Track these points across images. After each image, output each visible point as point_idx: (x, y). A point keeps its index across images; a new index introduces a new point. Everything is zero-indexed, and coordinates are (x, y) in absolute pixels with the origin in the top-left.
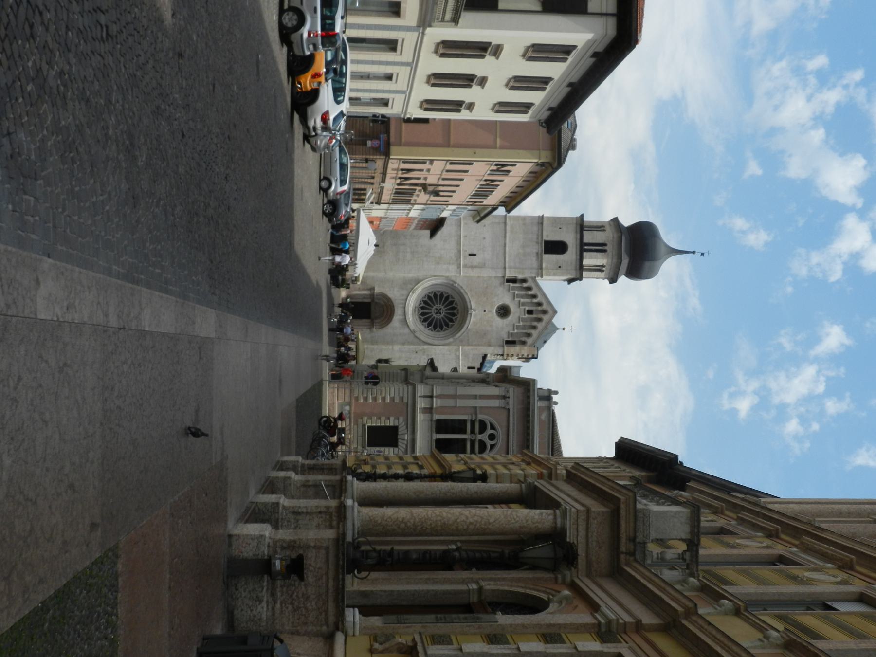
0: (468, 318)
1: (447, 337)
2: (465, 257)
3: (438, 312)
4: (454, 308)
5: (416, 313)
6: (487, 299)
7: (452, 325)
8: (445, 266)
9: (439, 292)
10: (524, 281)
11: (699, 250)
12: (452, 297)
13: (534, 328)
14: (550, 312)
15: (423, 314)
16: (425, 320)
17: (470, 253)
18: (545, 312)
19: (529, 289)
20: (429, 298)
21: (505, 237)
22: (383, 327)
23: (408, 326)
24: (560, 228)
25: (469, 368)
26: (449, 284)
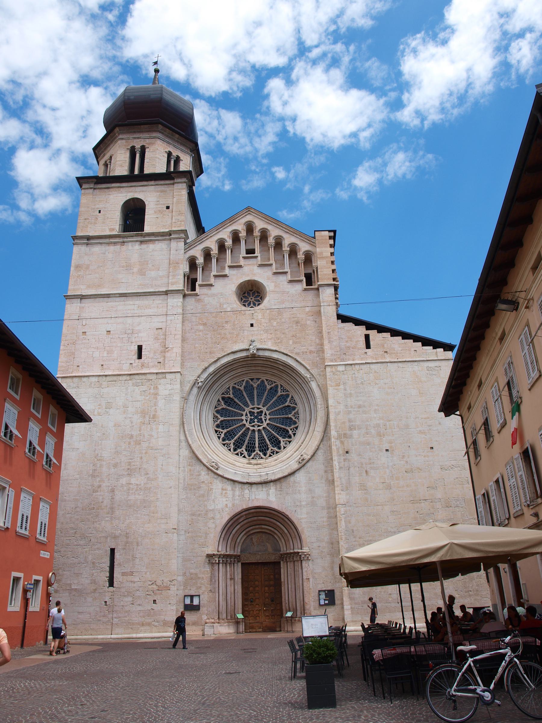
0: (267, 354)
1: (308, 394)
2: (143, 366)
3: (257, 416)
4: (249, 389)
6: (227, 322)
7: (284, 390)
8: (161, 403)
9: (215, 417)
12: (227, 392)
13: (278, 244)
15: (264, 449)
16: (277, 444)
17: (136, 356)
21: (108, 296)
24: (100, 212)
25: (368, 346)
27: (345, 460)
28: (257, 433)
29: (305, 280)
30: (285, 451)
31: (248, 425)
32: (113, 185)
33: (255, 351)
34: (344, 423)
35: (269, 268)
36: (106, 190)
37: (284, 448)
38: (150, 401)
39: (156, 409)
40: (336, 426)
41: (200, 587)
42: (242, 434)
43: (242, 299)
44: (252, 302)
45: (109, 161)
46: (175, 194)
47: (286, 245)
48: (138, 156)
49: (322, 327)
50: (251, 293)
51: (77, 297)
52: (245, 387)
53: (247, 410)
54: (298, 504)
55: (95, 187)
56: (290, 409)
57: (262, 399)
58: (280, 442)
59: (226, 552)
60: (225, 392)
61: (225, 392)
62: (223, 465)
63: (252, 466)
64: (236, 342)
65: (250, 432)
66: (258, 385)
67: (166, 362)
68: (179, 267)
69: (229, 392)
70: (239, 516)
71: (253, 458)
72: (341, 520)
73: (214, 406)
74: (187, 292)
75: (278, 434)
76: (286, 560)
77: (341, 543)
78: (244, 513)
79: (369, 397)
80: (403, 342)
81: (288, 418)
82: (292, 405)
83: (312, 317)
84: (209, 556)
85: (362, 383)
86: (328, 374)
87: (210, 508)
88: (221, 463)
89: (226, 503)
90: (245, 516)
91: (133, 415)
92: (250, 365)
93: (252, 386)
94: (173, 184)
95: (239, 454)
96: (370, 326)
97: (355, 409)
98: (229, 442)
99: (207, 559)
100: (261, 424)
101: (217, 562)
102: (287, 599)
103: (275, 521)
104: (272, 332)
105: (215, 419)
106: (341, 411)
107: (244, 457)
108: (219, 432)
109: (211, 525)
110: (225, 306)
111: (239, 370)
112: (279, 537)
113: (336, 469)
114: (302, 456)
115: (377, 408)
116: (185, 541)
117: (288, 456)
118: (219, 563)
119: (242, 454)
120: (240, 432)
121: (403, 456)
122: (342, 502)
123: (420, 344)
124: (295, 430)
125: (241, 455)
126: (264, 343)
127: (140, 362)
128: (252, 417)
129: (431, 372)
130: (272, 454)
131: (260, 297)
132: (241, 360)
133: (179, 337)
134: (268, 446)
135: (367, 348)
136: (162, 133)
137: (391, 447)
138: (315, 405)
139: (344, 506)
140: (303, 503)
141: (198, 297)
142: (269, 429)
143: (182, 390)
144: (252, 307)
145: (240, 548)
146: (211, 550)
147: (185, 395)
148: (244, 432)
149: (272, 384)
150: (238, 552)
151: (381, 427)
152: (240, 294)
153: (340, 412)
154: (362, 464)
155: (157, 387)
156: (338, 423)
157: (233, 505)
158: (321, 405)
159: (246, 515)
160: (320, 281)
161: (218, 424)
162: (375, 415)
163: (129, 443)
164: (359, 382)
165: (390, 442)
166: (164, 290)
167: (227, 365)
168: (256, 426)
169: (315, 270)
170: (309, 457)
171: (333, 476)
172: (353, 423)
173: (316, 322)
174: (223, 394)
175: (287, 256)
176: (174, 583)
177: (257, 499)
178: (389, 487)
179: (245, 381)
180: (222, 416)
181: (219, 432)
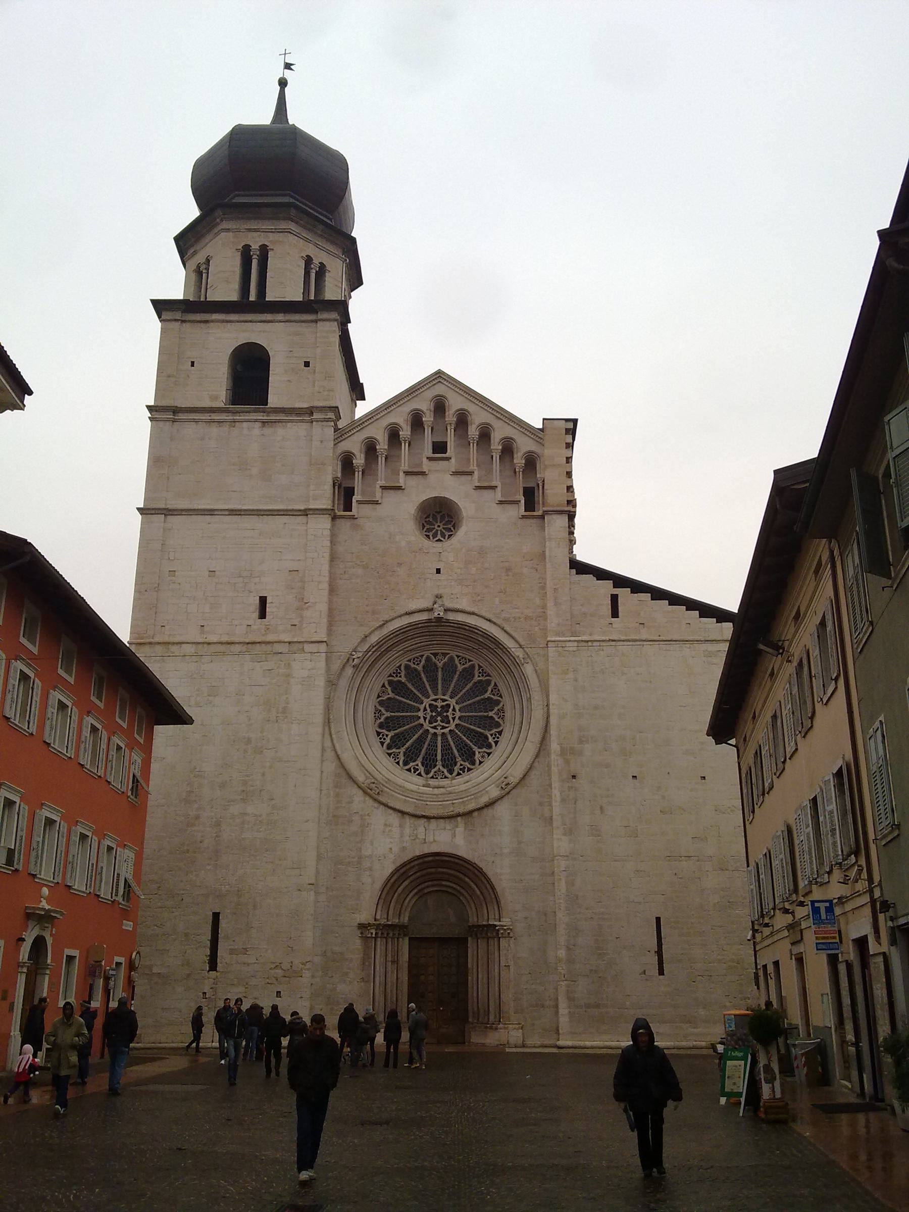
0: (460, 618)
1: (520, 685)
6: (400, 564)
7: (483, 673)
9: (378, 713)
10: (347, 462)
11: (280, 72)
12: (397, 673)
13: (485, 435)
14: (440, 390)
15: (450, 764)
16: (469, 756)
17: (257, 614)
18: (440, 407)
19: (371, 448)
20: (396, 742)
21: (211, 512)
22: (493, 888)
23: (491, 804)
24: (193, 364)
25: (615, 614)
28: (439, 738)
29: (523, 502)
30: (481, 769)
31: (426, 726)
32: (215, 316)
33: (442, 614)
35: (469, 477)
36: (202, 325)
37: (480, 764)
38: (279, 686)
39: (287, 698)
41: (347, 974)
43: (424, 526)
44: (439, 532)
45: (204, 266)
46: (318, 340)
47: (497, 440)
48: (255, 263)
49: (546, 579)
51: (159, 512)
52: (424, 667)
53: (427, 702)
55: (183, 319)
56: (491, 703)
58: (474, 753)
59: (388, 921)
60: (394, 673)
61: (394, 673)
62: (387, 788)
63: (431, 789)
65: (430, 736)
66: (444, 664)
67: (304, 625)
70: (408, 867)
71: (432, 777)
72: (560, 879)
74: (339, 513)
76: (476, 935)
77: (560, 915)
78: (416, 862)
80: (670, 610)
81: (487, 716)
82: (495, 698)
84: (362, 927)
86: (550, 655)
87: (366, 854)
88: (384, 784)
89: (390, 846)
91: (252, 707)
92: (432, 633)
93: (435, 664)
94: (316, 321)
95: (413, 770)
98: (398, 751)
99: (359, 932)
100: (447, 725)
101: (374, 936)
102: (475, 995)
103: (461, 876)
105: (377, 715)
107: (420, 774)
108: (383, 735)
109: (366, 879)
110: (397, 538)
111: (417, 640)
112: (467, 900)
113: (556, 801)
114: (505, 778)
116: (326, 903)
117: (486, 775)
118: (376, 938)
119: (416, 770)
121: (659, 788)
123: (696, 613)
124: (497, 735)
125: (415, 772)
127: (263, 623)
131: (452, 524)
132: (420, 625)
133: (325, 586)
134: (455, 760)
135: (612, 617)
136: (297, 223)
138: (529, 699)
139: (566, 858)
140: (506, 851)
141: (356, 521)
142: (459, 733)
143: (328, 669)
144: (439, 540)
145: (407, 914)
146: (365, 917)
148: (420, 736)
149: (466, 662)
150: (405, 919)
152: (421, 517)
153: (567, 715)
155: (289, 664)
159: (418, 865)
161: (381, 723)
163: (246, 751)
166: (302, 508)
167: (398, 633)
168: (439, 728)
169: (541, 485)
171: (551, 810)
173: (537, 570)
174: (390, 675)
175: (496, 457)
176: (308, 966)
179: (424, 657)
180: (387, 711)
181: (383, 735)
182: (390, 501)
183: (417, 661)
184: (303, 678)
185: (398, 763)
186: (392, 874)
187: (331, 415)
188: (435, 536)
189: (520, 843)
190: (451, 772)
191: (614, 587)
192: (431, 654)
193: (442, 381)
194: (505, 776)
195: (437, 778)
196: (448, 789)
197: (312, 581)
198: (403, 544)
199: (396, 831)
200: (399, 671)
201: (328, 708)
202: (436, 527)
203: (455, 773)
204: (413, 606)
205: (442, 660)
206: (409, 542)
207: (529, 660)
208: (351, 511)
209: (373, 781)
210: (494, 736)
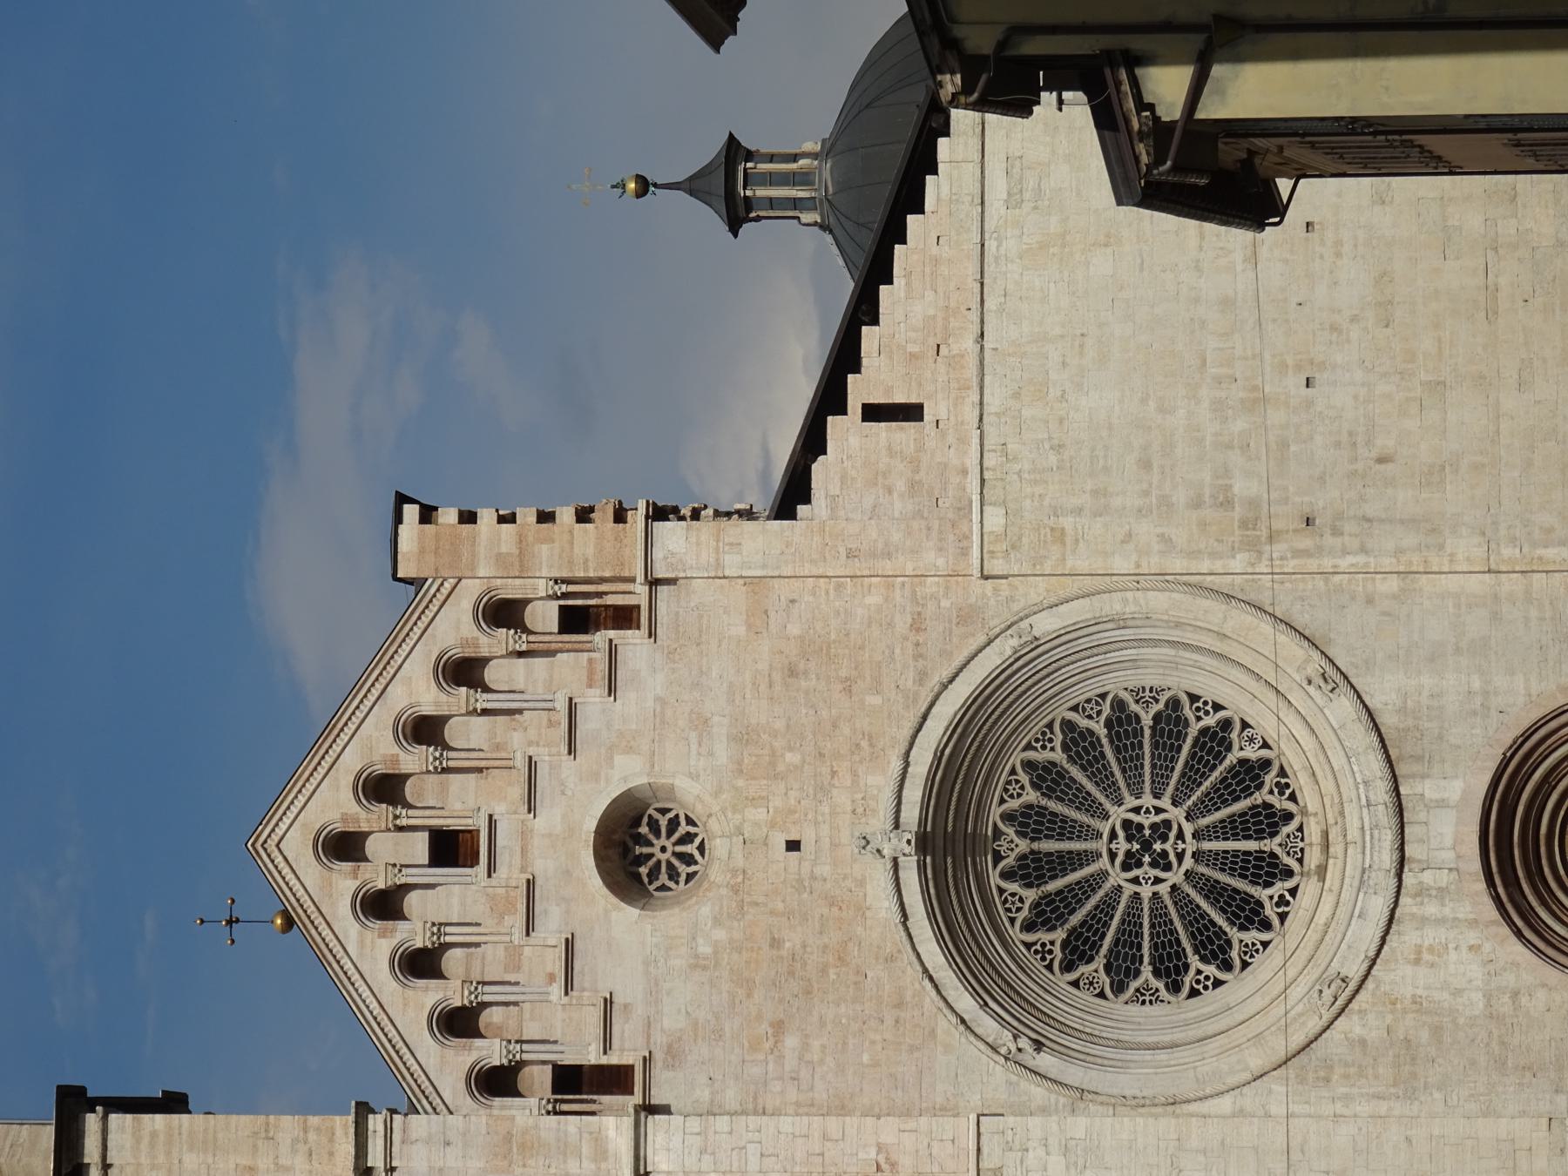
0: (914, 794)
5: (1313, 832)
6: (775, 943)
7: (1044, 740)
9: (1141, 997)
12: (1044, 951)
15: (1268, 821)
16: (1250, 773)
25: (911, 412)
26: (1064, 1053)
27: (1336, 532)
28: (1207, 845)
29: (612, 633)
31: (1175, 877)
34: (1203, 525)
37: (1269, 748)
40: (1214, 555)
42: (1206, 897)
44: (679, 849)
47: (443, 697)
50: (638, 850)
53: (1117, 877)
54: (1478, 700)
56: (1122, 721)
57: (1075, 821)
58: (1243, 762)
60: (1043, 959)
63: (1331, 861)
64: (862, 910)
65: (1202, 869)
68: (525, 1132)
69: (1044, 945)
71: (1300, 861)
72: (1540, 558)
73: (1098, 1001)
74: (637, 1098)
75: (1214, 767)
78: (1501, 890)
79: (1110, 428)
80: (903, 282)
81: (1153, 728)
82: (1107, 710)
83: (772, 614)
85: (1058, 448)
87: (1481, 1005)
89: (1464, 950)
90: (1511, 889)
93: (1023, 857)
96: (830, 399)
97: (1155, 482)
104: (825, 770)
105: (1147, 998)
106: (1159, 530)
107: (1293, 892)
110: (705, 949)
114: (1310, 682)
115: (1152, 404)
119: (1282, 901)
120: (1198, 907)
121: (1334, 328)
122: (1480, 552)
123: (912, 220)
124: (1200, 704)
125: (1287, 904)
126: (872, 804)
128: (1147, 859)
129: (1027, 196)
130: (1288, 792)
132: (932, 891)
133: (833, 1123)
134: (1258, 806)
135: (921, 419)
137: (1299, 368)
138: (1121, 623)
139: (1493, 546)
141: (658, 1056)
142: (1194, 798)
143: (1044, 1111)
144: (701, 848)
147: (1062, 1100)
148: (1200, 891)
149: (1017, 782)
151: (1223, 395)
153: (1163, 535)
154: (1354, 473)
156: (1202, 546)
157: (1473, 923)
158: (1125, 601)
159: (1506, 886)
160: (626, 574)
162: (1182, 412)
164: (1053, 459)
165: (1282, 368)
170: (1316, 655)
172: (1207, 492)
173: (793, 601)
174: (1049, 967)
177: (1455, 841)
178: (1438, 387)
179: (1003, 884)
180: (1137, 973)
181: (1198, 982)
182: (598, 974)
183: (1013, 903)
184: (1067, 1168)
185: (1265, 944)
186: (1528, 943)
187: (376, 1123)
188: (688, 859)
189: (1458, 650)
190: (1289, 817)
191: (842, 410)
192: (995, 866)
193: (275, 838)
194: (1305, 684)
195: (1302, 850)
196: (1331, 821)
197: (823, 1155)
198: (720, 934)
199: (1431, 936)
200: (1038, 947)
201: (1138, 1104)
202: (664, 857)
203: (1290, 806)
204: (885, 906)
205: (1012, 841)
206: (717, 922)
207: (1024, 624)
208: (631, 1068)
209: (1316, 995)
210: (1201, 714)
